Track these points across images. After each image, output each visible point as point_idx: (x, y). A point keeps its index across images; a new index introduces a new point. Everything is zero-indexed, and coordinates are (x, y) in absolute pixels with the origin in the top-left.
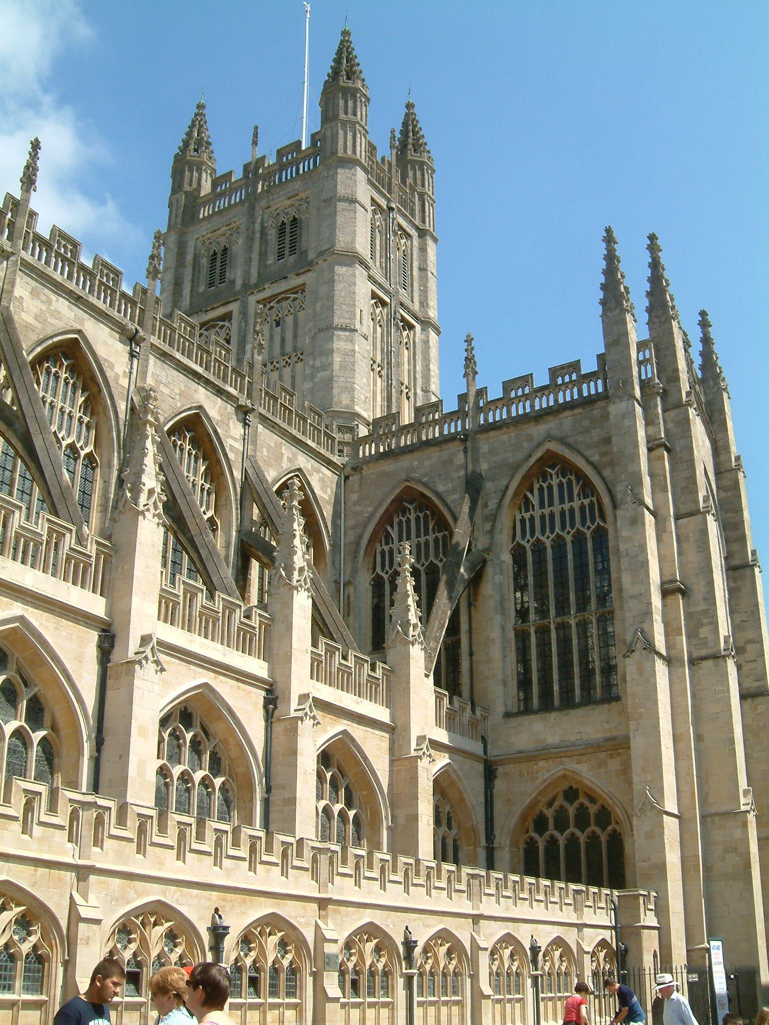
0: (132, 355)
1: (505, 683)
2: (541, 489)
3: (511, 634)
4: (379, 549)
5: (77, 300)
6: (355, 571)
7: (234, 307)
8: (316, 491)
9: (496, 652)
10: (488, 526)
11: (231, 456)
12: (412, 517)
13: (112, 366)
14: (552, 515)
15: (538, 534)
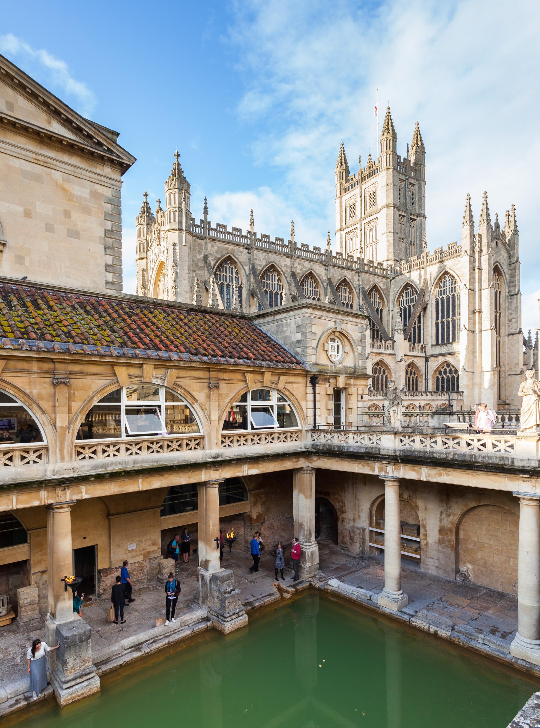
0: (326, 270)
1: (432, 337)
2: (444, 282)
3: (434, 324)
4: (400, 300)
5: (310, 260)
6: (394, 307)
7: (358, 226)
8: (382, 287)
9: (430, 329)
10: (429, 294)
11: (355, 286)
12: (409, 291)
13: (321, 275)
14: (446, 289)
15: (443, 295)
